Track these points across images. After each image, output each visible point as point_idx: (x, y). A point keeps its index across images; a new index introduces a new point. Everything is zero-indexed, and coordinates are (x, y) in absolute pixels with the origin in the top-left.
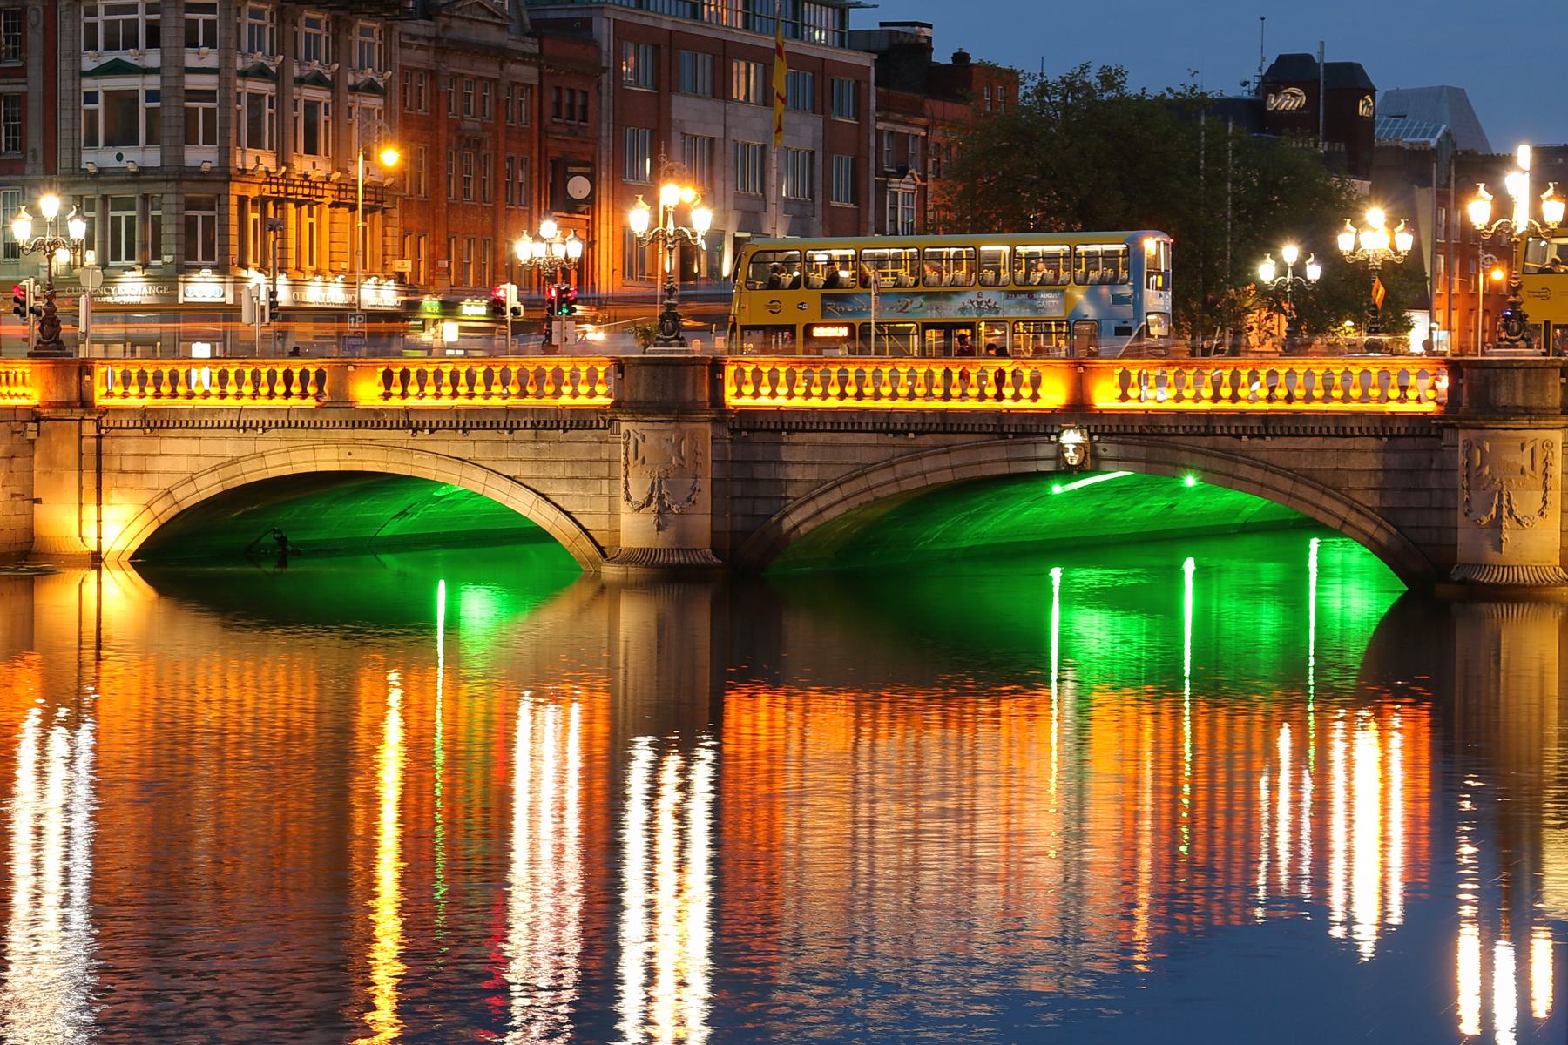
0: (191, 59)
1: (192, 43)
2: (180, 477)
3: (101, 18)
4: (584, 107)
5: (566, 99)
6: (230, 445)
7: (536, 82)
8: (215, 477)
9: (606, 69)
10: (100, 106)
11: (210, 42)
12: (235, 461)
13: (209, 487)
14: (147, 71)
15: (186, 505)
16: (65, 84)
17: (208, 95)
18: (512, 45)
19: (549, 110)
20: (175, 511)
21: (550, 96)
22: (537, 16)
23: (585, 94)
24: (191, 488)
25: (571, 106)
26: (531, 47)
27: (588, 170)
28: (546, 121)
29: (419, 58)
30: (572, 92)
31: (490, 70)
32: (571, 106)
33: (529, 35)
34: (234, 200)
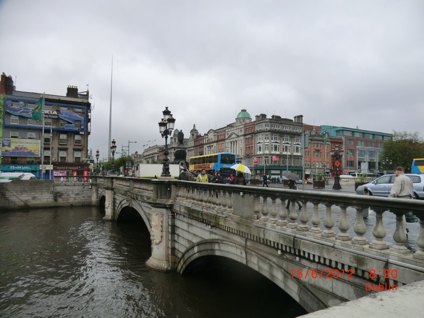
0: (266, 141)
1: (266, 139)
3: (259, 137)
10: (258, 147)
11: (268, 139)
14: (262, 143)
16: (256, 145)
17: (268, 145)
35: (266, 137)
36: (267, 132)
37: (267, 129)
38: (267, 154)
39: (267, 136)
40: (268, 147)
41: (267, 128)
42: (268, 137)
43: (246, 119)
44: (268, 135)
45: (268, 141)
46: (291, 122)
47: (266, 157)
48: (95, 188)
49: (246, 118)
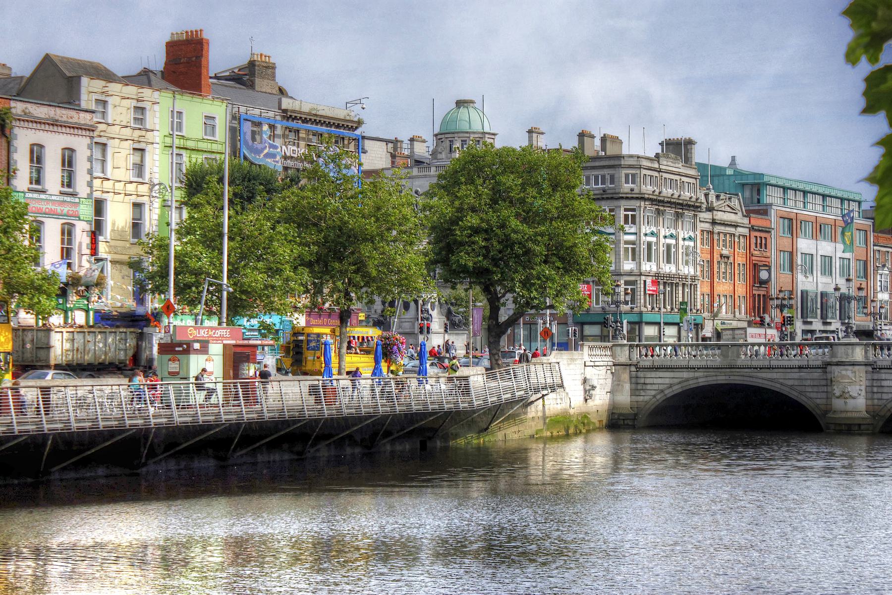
2: (666, 386)
4: (766, 245)
5: (759, 241)
6: (685, 375)
7: (748, 235)
8: (680, 386)
9: (773, 229)
11: (634, 222)
12: (687, 380)
13: (677, 389)
15: (668, 396)
17: (633, 243)
18: (739, 221)
19: (753, 246)
20: (665, 398)
21: (753, 240)
22: (747, 208)
23: (766, 238)
24: (671, 390)
25: (761, 244)
26: (746, 221)
27: (767, 268)
28: (752, 250)
29: (707, 226)
30: (761, 238)
31: (731, 230)
32: (761, 244)
33: (745, 216)
34: (642, 282)
35: (626, 217)
36: (632, 198)
37: (632, 190)
38: (630, 273)
39: (630, 213)
40: (633, 250)
41: (631, 185)
42: (633, 217)
43: (487, 136)
44: (634, 210)
45: (633, 230)
46: (677, 165)
47: (627, 283)
48: (628, 371)
49: (489, 134)
